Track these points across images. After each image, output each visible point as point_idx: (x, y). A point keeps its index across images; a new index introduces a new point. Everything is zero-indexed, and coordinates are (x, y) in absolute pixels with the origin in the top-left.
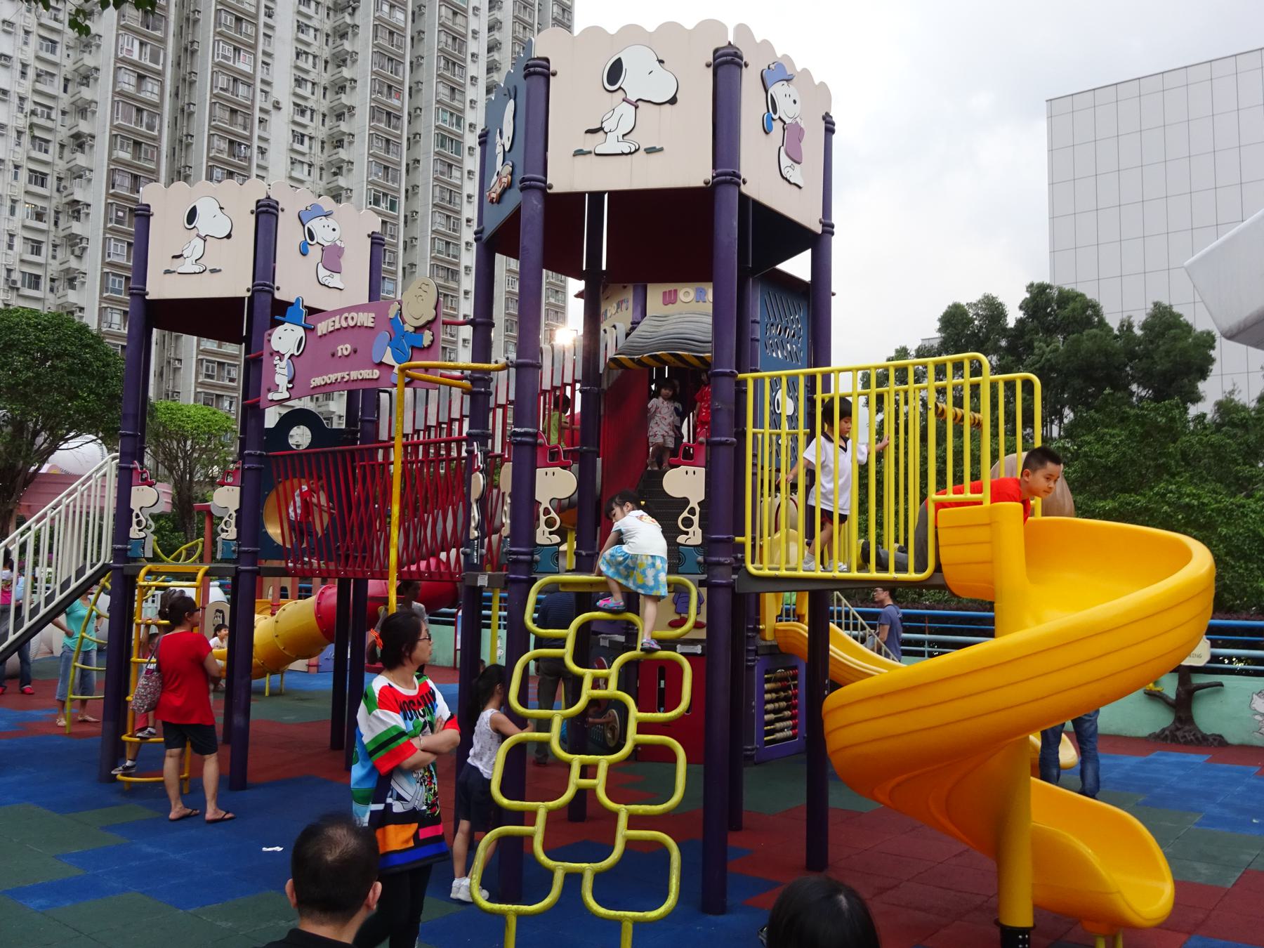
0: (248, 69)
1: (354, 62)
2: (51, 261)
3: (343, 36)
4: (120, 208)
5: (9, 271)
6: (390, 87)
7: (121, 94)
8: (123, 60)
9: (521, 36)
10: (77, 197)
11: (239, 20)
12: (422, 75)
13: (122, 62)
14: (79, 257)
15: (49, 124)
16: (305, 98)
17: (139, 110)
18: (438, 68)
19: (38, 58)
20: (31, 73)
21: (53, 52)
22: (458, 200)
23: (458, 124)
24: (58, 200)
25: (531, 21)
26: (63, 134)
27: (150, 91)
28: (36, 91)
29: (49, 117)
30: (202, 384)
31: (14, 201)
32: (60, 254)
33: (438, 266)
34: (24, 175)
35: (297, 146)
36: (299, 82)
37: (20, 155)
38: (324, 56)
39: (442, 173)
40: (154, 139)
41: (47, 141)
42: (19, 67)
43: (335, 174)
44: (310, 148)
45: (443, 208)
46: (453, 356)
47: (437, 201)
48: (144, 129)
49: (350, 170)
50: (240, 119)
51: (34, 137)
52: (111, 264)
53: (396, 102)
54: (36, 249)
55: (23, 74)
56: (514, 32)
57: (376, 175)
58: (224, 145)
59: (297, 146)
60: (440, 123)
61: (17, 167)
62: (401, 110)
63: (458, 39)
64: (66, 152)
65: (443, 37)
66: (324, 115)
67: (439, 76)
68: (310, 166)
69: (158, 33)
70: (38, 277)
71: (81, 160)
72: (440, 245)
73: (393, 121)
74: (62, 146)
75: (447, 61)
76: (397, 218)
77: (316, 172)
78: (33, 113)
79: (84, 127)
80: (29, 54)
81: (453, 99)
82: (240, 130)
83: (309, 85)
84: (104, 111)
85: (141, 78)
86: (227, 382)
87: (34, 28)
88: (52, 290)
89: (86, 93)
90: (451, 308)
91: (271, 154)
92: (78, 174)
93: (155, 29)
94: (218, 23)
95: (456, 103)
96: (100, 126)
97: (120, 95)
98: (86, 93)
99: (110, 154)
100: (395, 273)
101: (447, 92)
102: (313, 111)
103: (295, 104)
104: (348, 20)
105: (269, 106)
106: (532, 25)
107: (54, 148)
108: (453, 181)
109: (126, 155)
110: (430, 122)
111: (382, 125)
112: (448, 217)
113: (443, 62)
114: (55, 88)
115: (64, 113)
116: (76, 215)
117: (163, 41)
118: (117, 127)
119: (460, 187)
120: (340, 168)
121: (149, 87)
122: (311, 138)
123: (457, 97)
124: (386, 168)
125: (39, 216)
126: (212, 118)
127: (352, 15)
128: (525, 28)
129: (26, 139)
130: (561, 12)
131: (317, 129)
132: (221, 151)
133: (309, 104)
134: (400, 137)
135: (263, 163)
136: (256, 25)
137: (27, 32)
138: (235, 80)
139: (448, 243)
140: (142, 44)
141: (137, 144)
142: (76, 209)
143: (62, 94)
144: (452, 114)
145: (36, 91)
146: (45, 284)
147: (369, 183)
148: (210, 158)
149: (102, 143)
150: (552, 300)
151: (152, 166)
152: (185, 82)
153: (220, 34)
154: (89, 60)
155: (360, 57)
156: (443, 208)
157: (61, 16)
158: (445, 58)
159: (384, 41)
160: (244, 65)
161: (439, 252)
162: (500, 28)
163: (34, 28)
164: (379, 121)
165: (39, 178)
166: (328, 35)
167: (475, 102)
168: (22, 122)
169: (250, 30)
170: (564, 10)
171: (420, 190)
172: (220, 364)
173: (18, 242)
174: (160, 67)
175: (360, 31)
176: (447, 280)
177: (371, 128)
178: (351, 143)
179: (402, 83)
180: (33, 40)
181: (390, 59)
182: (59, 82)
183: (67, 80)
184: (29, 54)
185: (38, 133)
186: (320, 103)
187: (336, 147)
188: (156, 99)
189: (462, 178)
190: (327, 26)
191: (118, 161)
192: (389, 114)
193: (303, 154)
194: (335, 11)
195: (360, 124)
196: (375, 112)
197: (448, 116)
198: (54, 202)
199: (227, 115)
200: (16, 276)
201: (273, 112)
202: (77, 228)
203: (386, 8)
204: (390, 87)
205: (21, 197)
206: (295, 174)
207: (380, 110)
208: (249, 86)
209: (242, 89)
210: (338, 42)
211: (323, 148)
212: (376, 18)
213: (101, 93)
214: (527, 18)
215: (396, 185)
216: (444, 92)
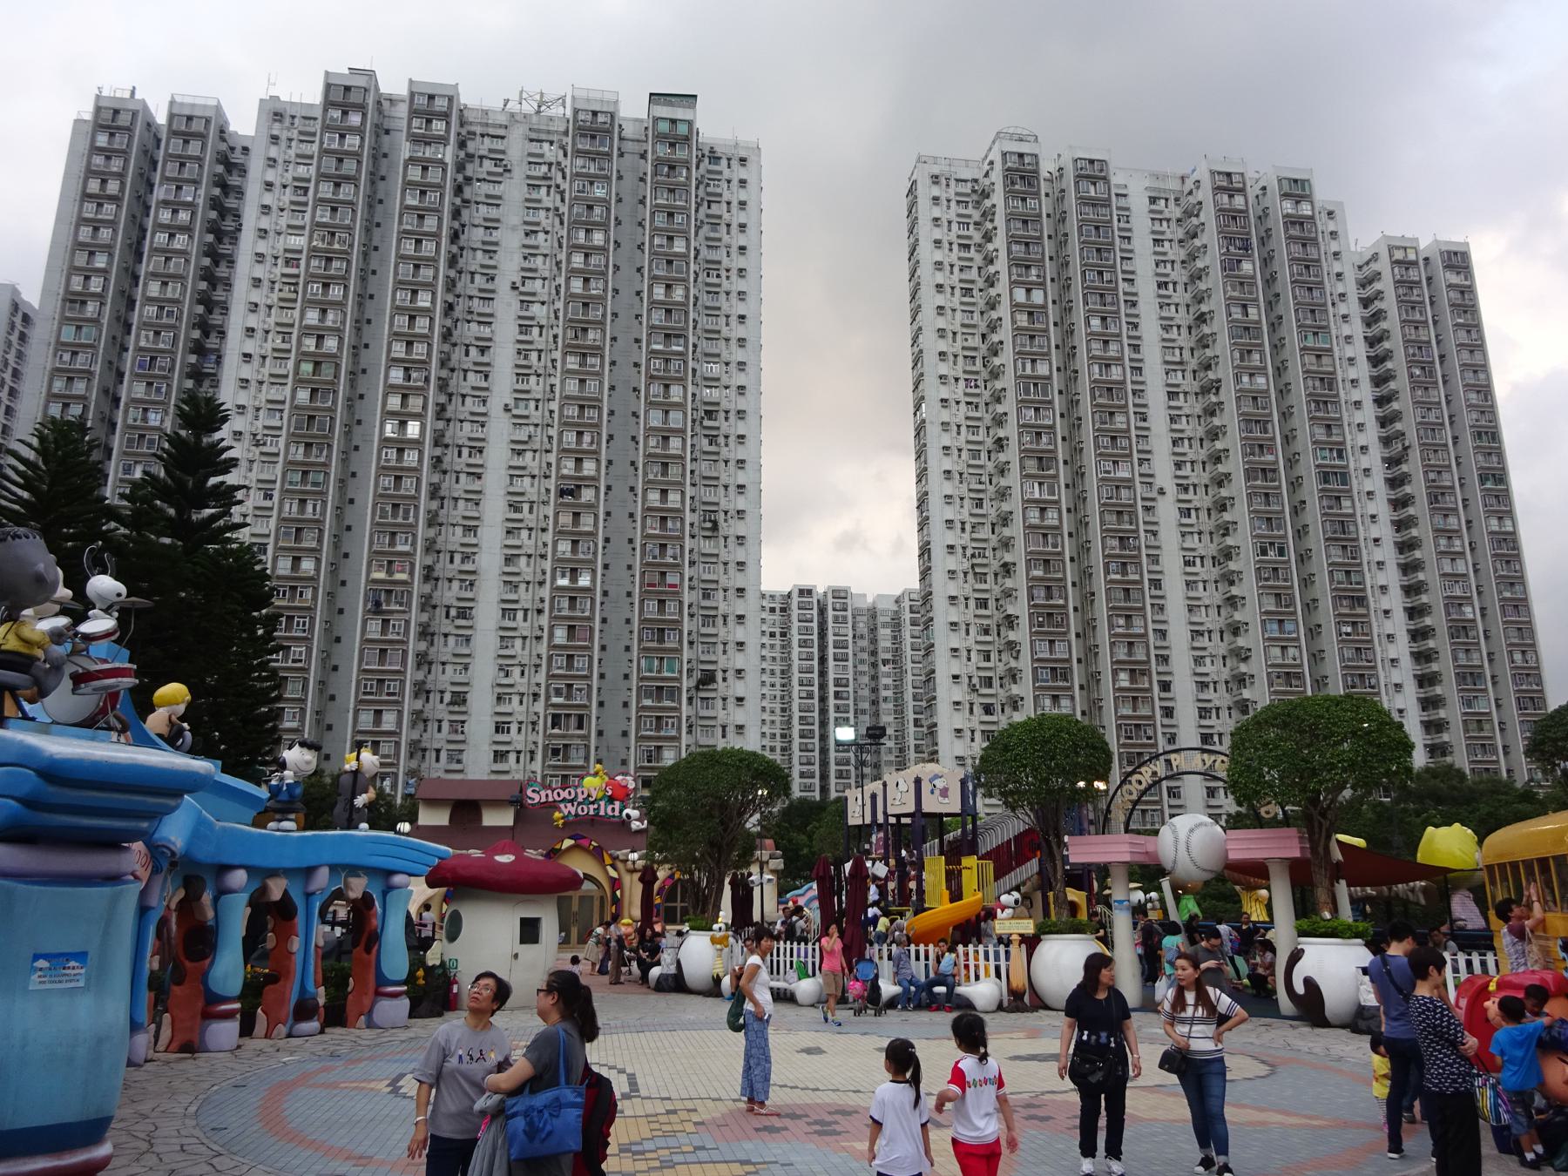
0: (1126, 475)
1: (1225, 433)
2: (998, 664)
3: (1213, 414)
4: (1039, 615)
5: (970, 677)
6: (1261, 446)
7: (1031, 527)
8: (1029, 501)
9: (1413, 337)
10: (1009, 612)
11: (1114, 438)
12: (1295, 422)
13: (1028, 503)
14: (1016, 658)
15: (985, 561)
16: (1186, 477)
17: (1045, 535)
18: (1309, 412)
19: (971, 515)
20: (968, 527)
21: (981, 507)
22: (1352, 528)
23: (1340, 456)
24: (998, 616)
25: (1423, 319)
26: (995, 565)
27: (1052, 518)
28: (973, 540)
29: (984, 557)
30: (1124, 745)
31: (968, 625)
32: (1005, 657)
33: (1340, 597)
34: (972, 603)
35: (1185, 521)
36: (1178, 465)
37: (968, 590)
38: (1198, 436)
39: (1330, 507)
40: (1059, 554)
41: (985, 574)
42: (959, 525)
43: (1224, 535)
44: (1198, 518)
45: (1336, 539)
46: (1373, 681)
47: (1329, 535)
48: (1050, 549)
49: (1235, 530)
50: (1126, 518)
51: (975, 574)
52: (1039, 660)
53: (1270, 458)
54: (988, 659)
55: (963, 530)
56: (1404, 336)
57: (1260, 528)
58: (1115, 543)
59: (1185, 521)
60: (1320, 461)
61: (966, 599)
62: (1276, 462)
63: (1328, 380)
64: (999, 577)
65: (1310, 383)
66: (1206, 486)
67: (1311, 419)
68: (1200, 533)
69: (1052, 472)
70: (991, 678)
71: (1009, 583)
72: (1340, 576)
73: (1269, 475)
74: (996, 575)
75: (1317, 402)
76: (1289, 561)
77: (1206, 538)
78: (973, 556)
79: (1008, 558)
80: (965, 515)
81: (1329, 434)
82: (1128, 527)
83: (1188, 465)
84: (1020, 543)
85: (1043, 510)
86: (1145, 741)
87: (966, 494)
88: (1001, 686)
89: (1007, 532)
90: (1363, 634)
91: (1162, 535)
92: (1008, 594)
93: (1048, 469)
94: (1097, 446)
95: (1334, 438)
96: (1017, 555)
97: (1030, 528)
98: (1007, 532)
99: (1027, 574)
100: (1294, 613)
101: (1323, 431)
102: (1195, 486)
103: (1178, 485)
104: (1214, 399)
105: (1154, 494)
106: (1426, 322)
107: (990, 578)
108: (1344, 511)
109: (1038, 573)
110: (1308, 467)
111: (1259, 482)
112: (1344, 547)
113: (1313, 405)
114: (984, 533)
115: (994, 549)
116: (1011, 627)
117: (1056, 477)
118: (1030, 553)
119: (1353, 515)
120: (1227, 529)
121: (1050, 515)
122: (1197, 510)
123: (1334, 431)
124: (1269, 519)
125: (986, 632)
126: (1102, 523)
127: (1217, 393)
128: (1416, 328)
129: (970, 577)
130: (1459, 296)
131: (1201, 500)
132: (1113, 548)
133: (1190, 482)
134: (1279, 487)
135: (1153, 543)
136: (1129, 438)
137: (962, 499)
138: (1117, 487)
139: (1348, 573)
140: (1040, 484)
141: (1047, 562)
142: (1010, 621)
143: (991, 536)
144: (1331, 450)
145: (973, 540)
146: (996, 683)
147: (1253, 537)
148: (1105, 556)
149: (1021, 568)
150: (1507, 595)
151: (1060, 575)
152: (1080, 499)
153: (1100, 454)
154: (1005, 507)
155: (1228, 429)
156: (1336, 539)
157: (983, 479)
158: (1315, 401)
159: (1248, 408)
160: (1123, 473)
161: (1339, 583)
162: (1388, 338)
163: (966, 494)
164: (1256, 479)
165: (983, 604)
166: (1199, 417)
167: (1363, 425)
168: (966, 565)
169: (1125, 443)
170: (1462, 293)
171: (1311, 528)
172: (1136, 725)
173: (973, 655)
174: (1056, 497)
175: (1226, 406)
176: (1353, 607)
177: (1247, 488)
178: (1233, 505)
179: (1273, 439)
180: (967, 502)
181: (1257, 422)
182: (988, 528)
183: (993, 525)
184: (965, 515)
185: (978, 570)
186: (1200, 477)
187: (1220, 511)
188: (1056, 523)
189: (1353, 506)
190: (1198, 410)
191: (1035, 579)
192: (1264, 470)
193: (1192, 525)
194: (1203, 393)
195: (1238, 487)
196: (1250, 474)
197: (1327, 453)
198: (995, 618)
199: (1115, 517)
200: (975, 680)
201: (1159, 498)
202: (1012, 636)
203: (1246, 379)
204: (1261, 446)
205: (973, 621)
206: (1185, 546)
207: (1255, 470)
208: (1129, 488)
209: (1124, 493)
210: (1209, 419)
211: (1209, 515)
212: (1237, 391)
213: (1016, 530)
214: (1418, 317)
215: (1282, 532)
216: (1320, 433)
